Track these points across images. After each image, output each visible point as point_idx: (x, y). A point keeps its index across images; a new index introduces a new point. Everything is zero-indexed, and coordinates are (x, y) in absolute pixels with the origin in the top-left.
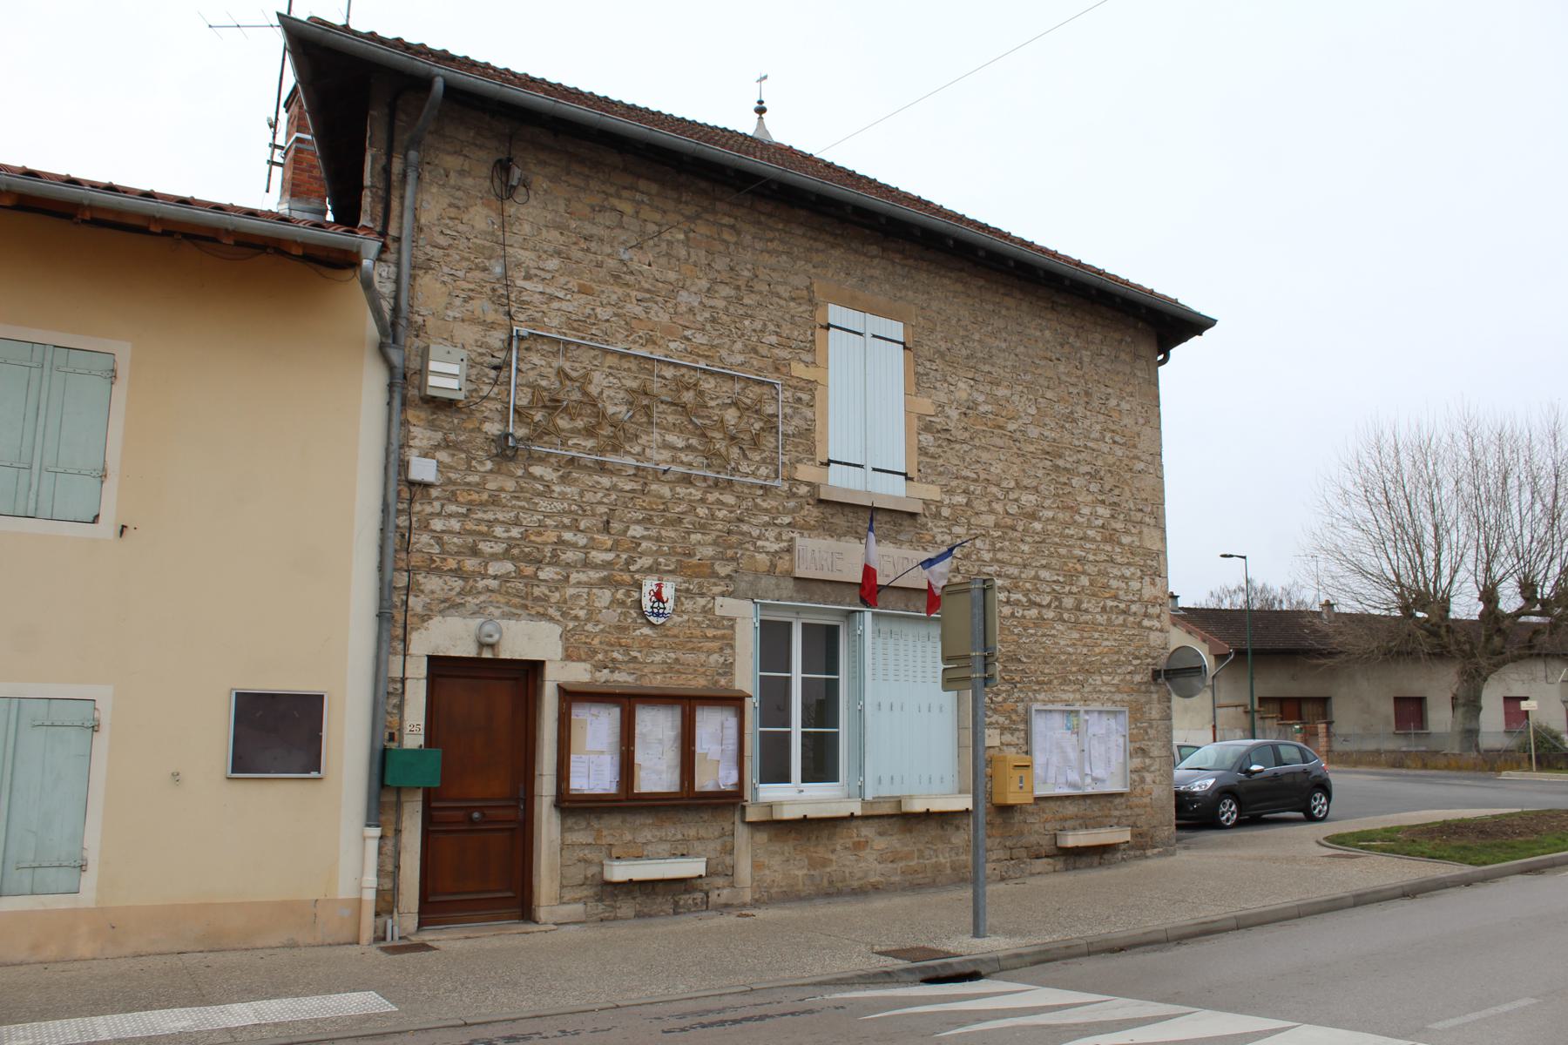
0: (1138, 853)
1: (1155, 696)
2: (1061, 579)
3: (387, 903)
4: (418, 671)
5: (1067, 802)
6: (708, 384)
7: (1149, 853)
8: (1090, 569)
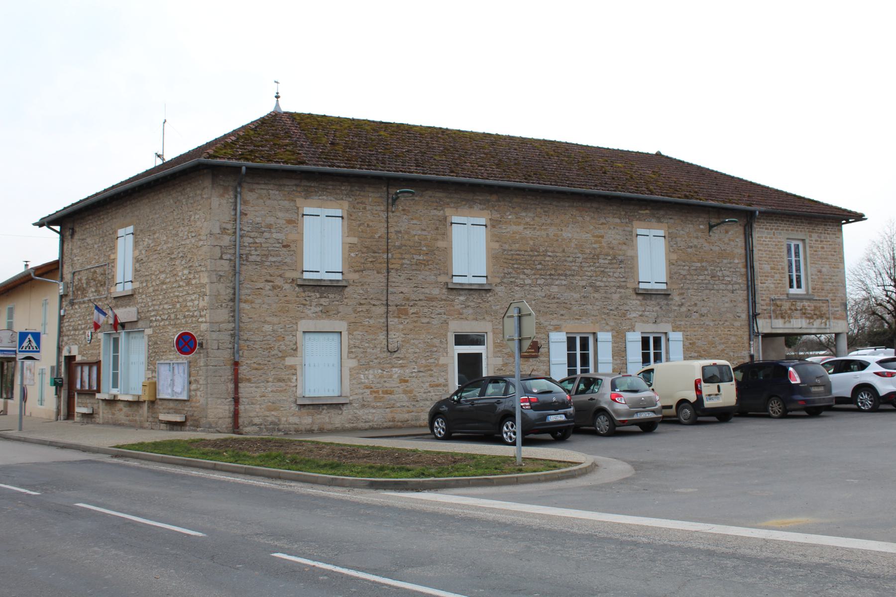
0: (194, 428)
1: (202, 355)
2: (171, 307)
3: (58, 413)
4: (63, 359)
5: (171, 402)
6: (98, 270)
7: (198, 429)
8: (181, 300)
